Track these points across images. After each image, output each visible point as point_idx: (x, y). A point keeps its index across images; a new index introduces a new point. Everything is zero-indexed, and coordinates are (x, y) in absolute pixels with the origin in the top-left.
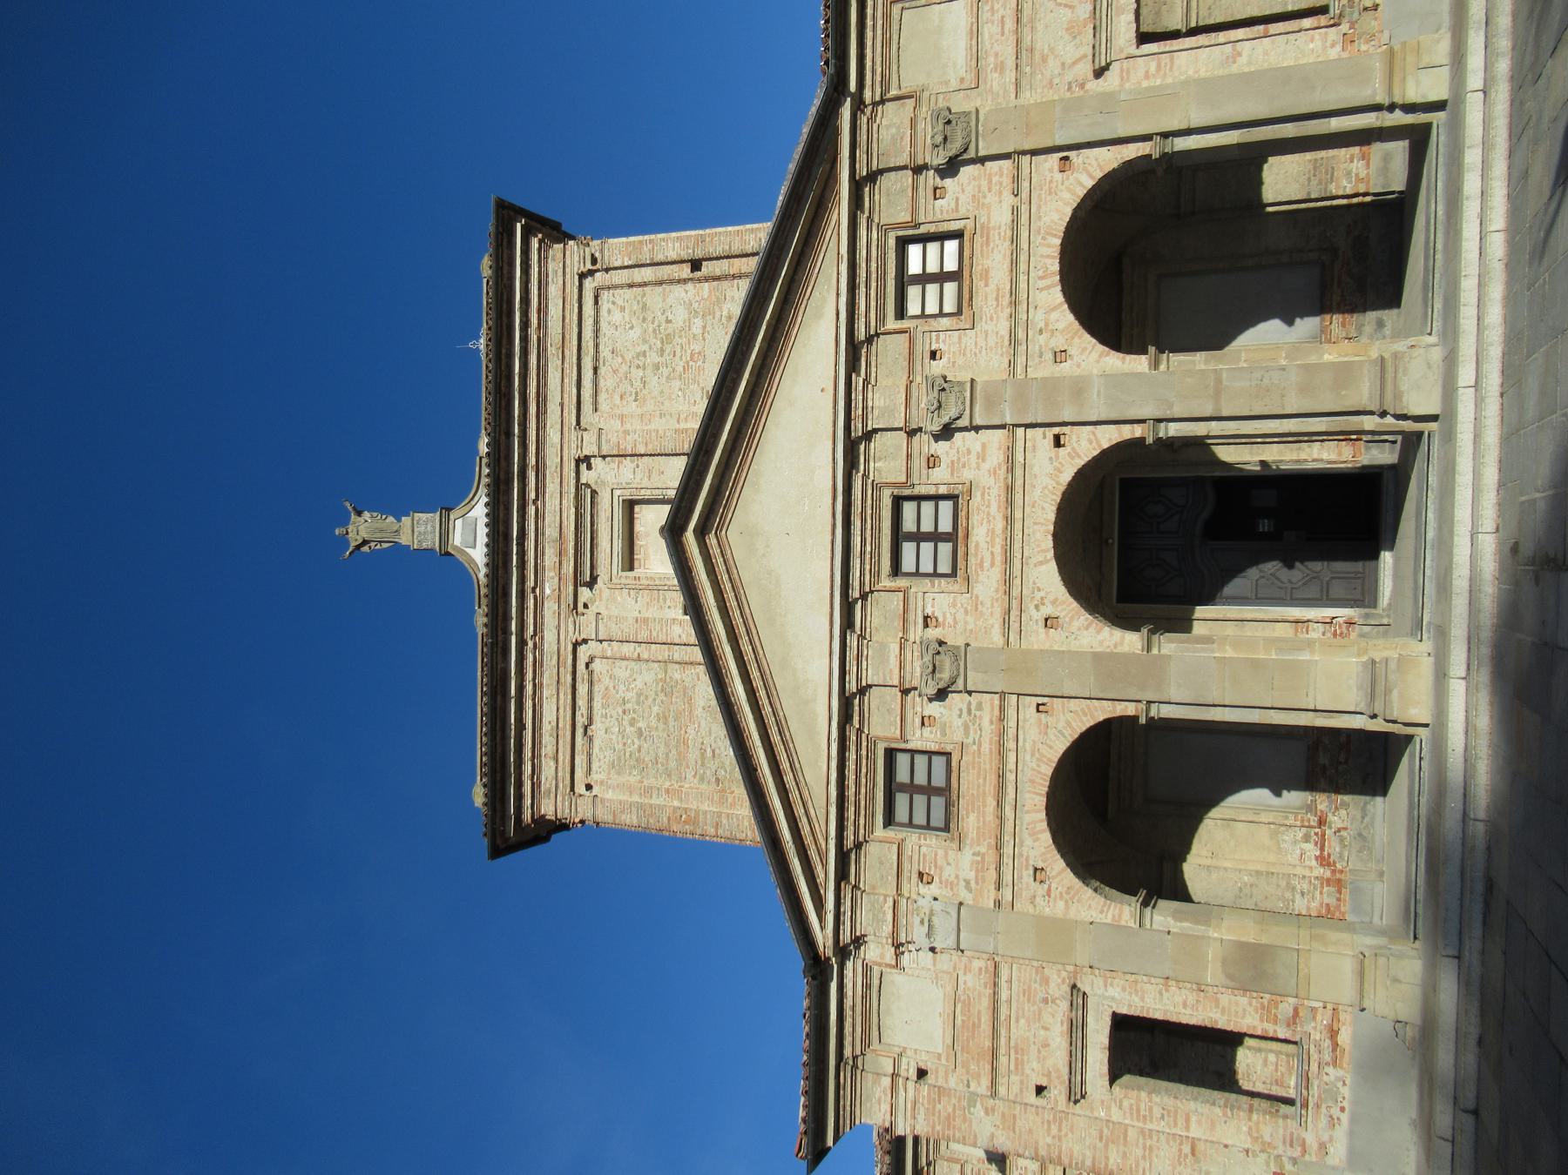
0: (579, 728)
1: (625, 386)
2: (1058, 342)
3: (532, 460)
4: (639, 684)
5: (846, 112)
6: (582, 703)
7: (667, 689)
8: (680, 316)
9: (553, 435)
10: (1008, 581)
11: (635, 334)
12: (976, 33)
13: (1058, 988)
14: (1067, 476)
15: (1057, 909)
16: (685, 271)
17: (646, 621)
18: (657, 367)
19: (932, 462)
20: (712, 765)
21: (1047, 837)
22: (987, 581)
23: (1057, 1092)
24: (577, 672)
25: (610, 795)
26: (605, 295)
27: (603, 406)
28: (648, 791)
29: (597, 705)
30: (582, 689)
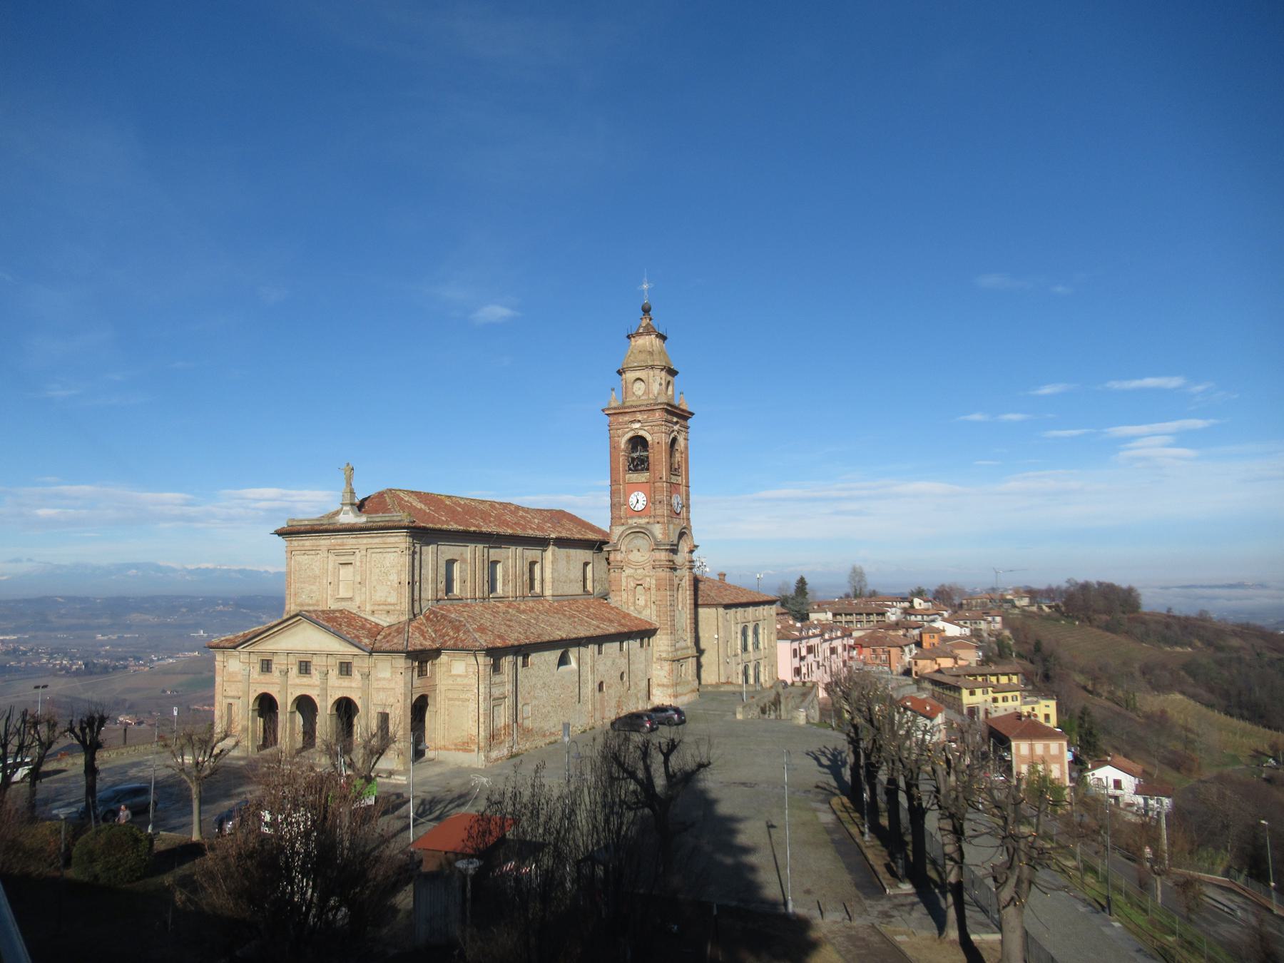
0: (305, 552)
1: (377, 561)
2: (333, 696)
3: (358, 536)
4: (316, 569)
5: (366, 654)
6: (311, 552)
7: (315, 577)
8: (391, 578)
9: (365, 541)
10: (297, 685)
11: (388, 565)
12: (384, 679)
13: (240, 694)
14: (313, 697)
15: (250, 694)
16: (399, 580)
17: (327, 572)
18: (381, 571)
19: (316, 670)
20: (300, 591)
21: (261, 692)
22: (298, 681)
23: (225, 694)
24: (316, 550)
25: (293, 562)
26: (396, 554)
27: (373, 555)
28: (294, 573)
29: (311, 556)
30: (313, 552)
